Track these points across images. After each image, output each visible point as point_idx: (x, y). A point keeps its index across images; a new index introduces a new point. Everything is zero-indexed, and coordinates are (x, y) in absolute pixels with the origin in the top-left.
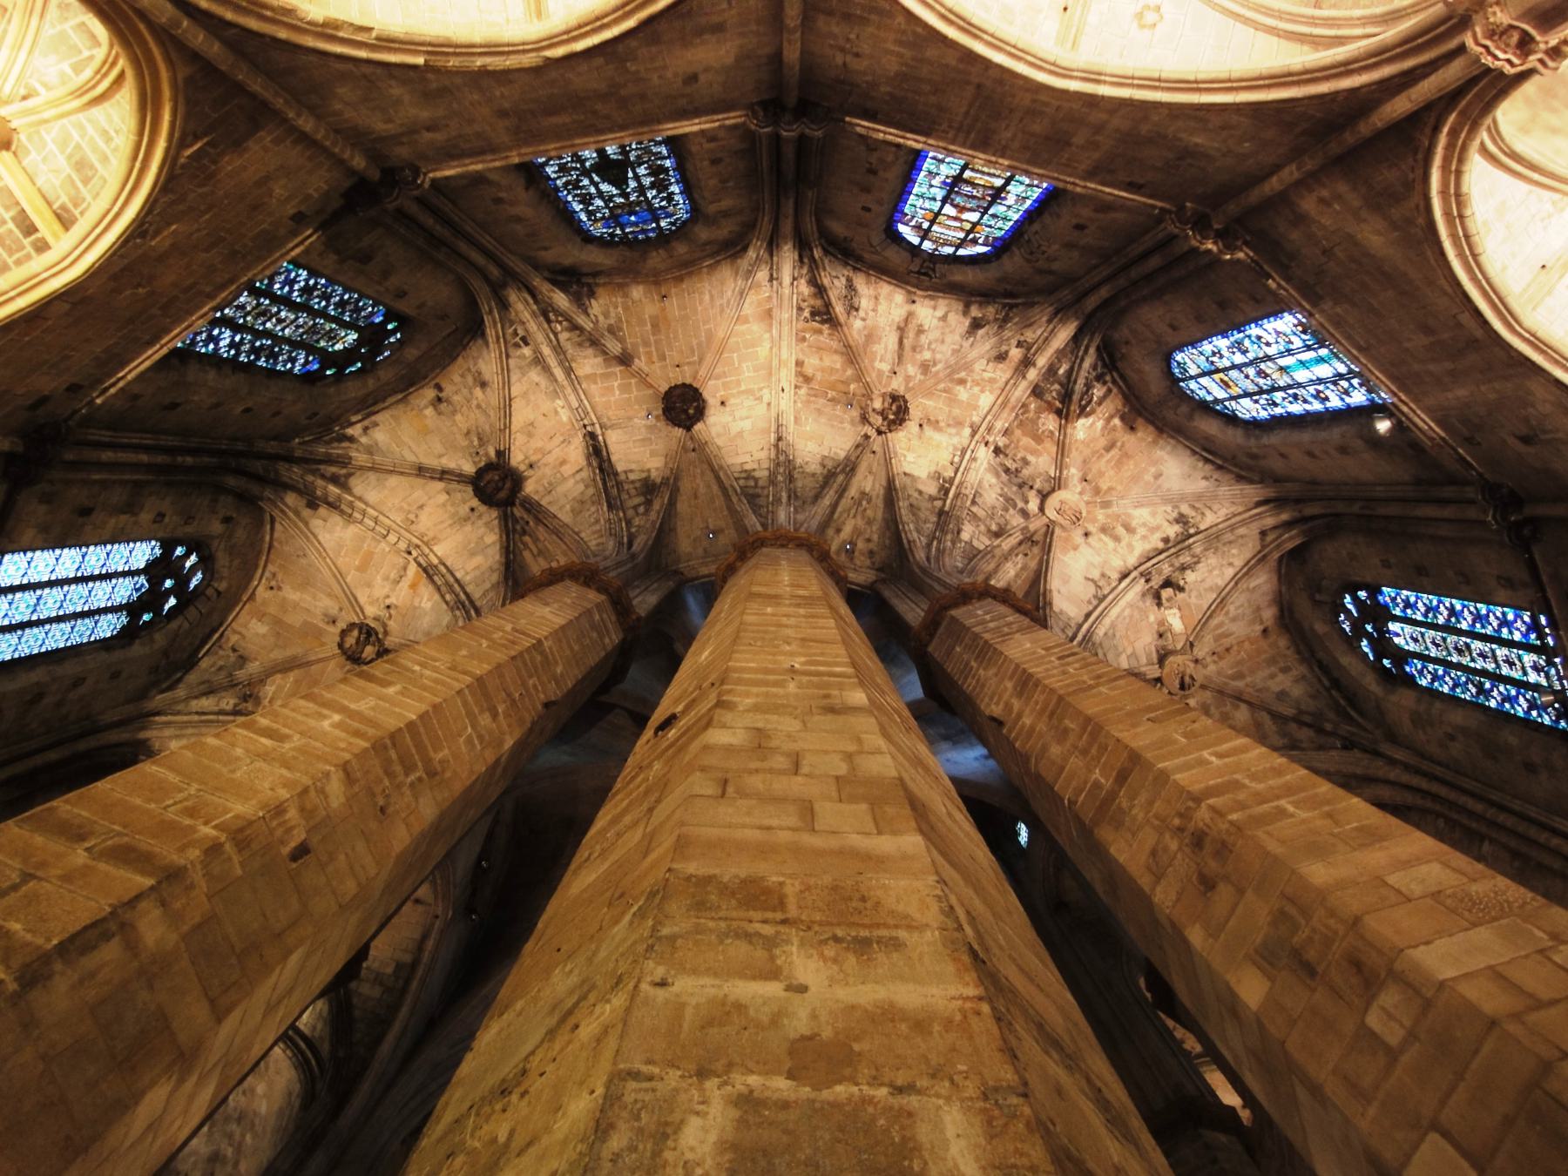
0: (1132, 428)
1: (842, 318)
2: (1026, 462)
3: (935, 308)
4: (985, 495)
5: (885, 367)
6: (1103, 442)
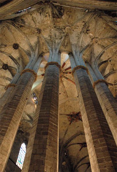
0: (71, 12)
1: (24, 25)
2: (60, 26)
3: (35, 14)
4: (57, 34)
5: (34, 26)
6: (68, 17)
